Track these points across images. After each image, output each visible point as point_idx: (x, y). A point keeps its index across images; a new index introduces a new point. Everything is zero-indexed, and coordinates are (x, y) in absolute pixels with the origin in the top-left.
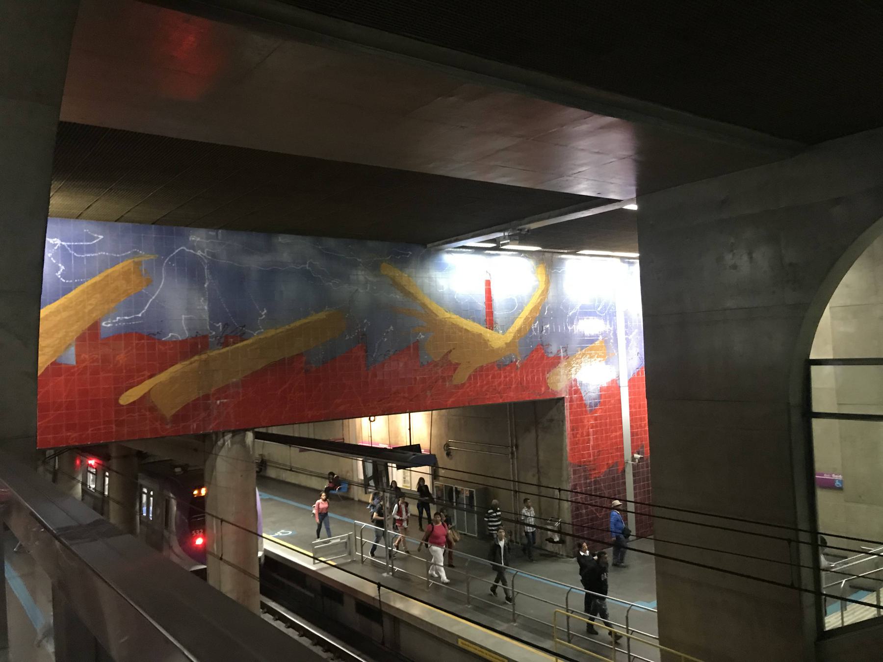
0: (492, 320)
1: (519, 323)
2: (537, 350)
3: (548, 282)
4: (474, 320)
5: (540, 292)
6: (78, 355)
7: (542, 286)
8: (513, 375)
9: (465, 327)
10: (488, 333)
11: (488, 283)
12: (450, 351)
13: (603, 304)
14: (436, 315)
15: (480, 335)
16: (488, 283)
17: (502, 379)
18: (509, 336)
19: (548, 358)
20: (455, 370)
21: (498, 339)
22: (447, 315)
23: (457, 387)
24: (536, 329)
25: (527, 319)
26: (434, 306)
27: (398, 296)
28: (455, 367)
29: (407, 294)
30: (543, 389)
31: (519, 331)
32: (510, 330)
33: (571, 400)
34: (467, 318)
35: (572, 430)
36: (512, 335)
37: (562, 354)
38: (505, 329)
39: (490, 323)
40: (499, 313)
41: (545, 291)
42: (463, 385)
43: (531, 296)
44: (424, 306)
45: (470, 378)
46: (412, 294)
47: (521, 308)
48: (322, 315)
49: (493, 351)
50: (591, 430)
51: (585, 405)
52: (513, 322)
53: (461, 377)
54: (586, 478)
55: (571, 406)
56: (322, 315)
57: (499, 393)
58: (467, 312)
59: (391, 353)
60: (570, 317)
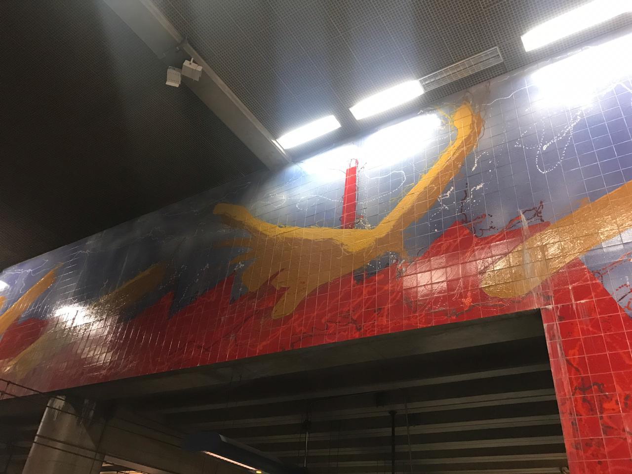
0: (354, 215)
3: (478, 124)
4: (321, 225)
9: (304, 237)
12: (277, 273)
14: (266, 236)
15: (329, 241)
17: (365, 296)
18: (384, 228)
20: (280, 296)
22: (283, 230)
24: (445, 202)
25: (427, 191)
32: (387, 218)
33: (566, 313)
34: (309, 226)
35: (582, 386)
36: (393, 223)
38: (375, 220)
40: (366, 203)
42: (288, 318)
43: (433, 159)
45: (301, 306)
48: (147, 272)
49: (350, 257)
52: (394, 205)
53: (285, 307)
55: (566, 330)
56: (147, 272)
57: (355, 322)
59: (199, 294)
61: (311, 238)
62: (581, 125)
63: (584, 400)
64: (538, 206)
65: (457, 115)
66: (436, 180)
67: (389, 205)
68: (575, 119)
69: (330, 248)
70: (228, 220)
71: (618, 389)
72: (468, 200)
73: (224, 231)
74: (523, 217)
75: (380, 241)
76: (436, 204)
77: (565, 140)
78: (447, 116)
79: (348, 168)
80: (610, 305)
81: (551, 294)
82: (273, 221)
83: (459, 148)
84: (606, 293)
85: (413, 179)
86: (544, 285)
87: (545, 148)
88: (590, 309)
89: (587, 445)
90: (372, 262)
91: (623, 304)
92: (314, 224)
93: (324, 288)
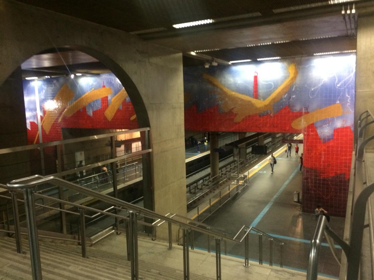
1: (274, 95)
2: (285, 109)
3: (296, 73)
4: (247, 95)
5: (290, 78)
6: (122, 107)
7: (292, 75)
8: (268, 120)
9: (242, 98)
10: (254, 101)
11: (256, 77)
13: (342, 82)
15: (250, 102)
16: (256, 77)
17: (261, 121)
19: (293, 113)
21: (259, 104)
23: (236, 123)
24: (285, 98)
25: (280, 93)
26: (226, 90)
27: (210, 86)
28: (236, 115)
29: (214, 85)
30: (288, 128)
31: (274, 99)
32: (268, 99)
34: (243, 93)
37: (304, 111)
38: (264, 99)
39: (256, 95)
40: (261, 91)
41: (295, 78)
42: (239, 123)
43: (282, 82)
44: (221, 90)
46: (216, 85)
47: (276, 87)
49: (257, 108)
50: (323, 153)
51: (320, 139)
52: (270, 95)
54: (316, 176)
57: (259, 127)
58: (244, 91)
60: (312, 91)
61: (243, 98)
62: (322, 85)
63: (308, 152)
64: (307, 107)
65: (290, 68)
66: (283, 89)
67: (269, 94)
68: (322, 83)
69: (250, 104)
70: (211, 83)
71: (314, 151)
72: (290, 100)
73: (210, 86)
74: (303, 109)
75: (266, 106)
76: (282, 99)
77: (317, 89)
78: (287, 66)
79: (254, 75)
80: (317, 135)
81: (306, 130)
82: (228, 88)
83: (290, 81)
84: (317, 132)
85: (276, 87)
86: (305, 128)
87: (313, 89)
88: (313, 135)
89: (307, 160)
90: (263, 112)
91: (319, 135)
92: (244, 94)
93: (249, 116)
